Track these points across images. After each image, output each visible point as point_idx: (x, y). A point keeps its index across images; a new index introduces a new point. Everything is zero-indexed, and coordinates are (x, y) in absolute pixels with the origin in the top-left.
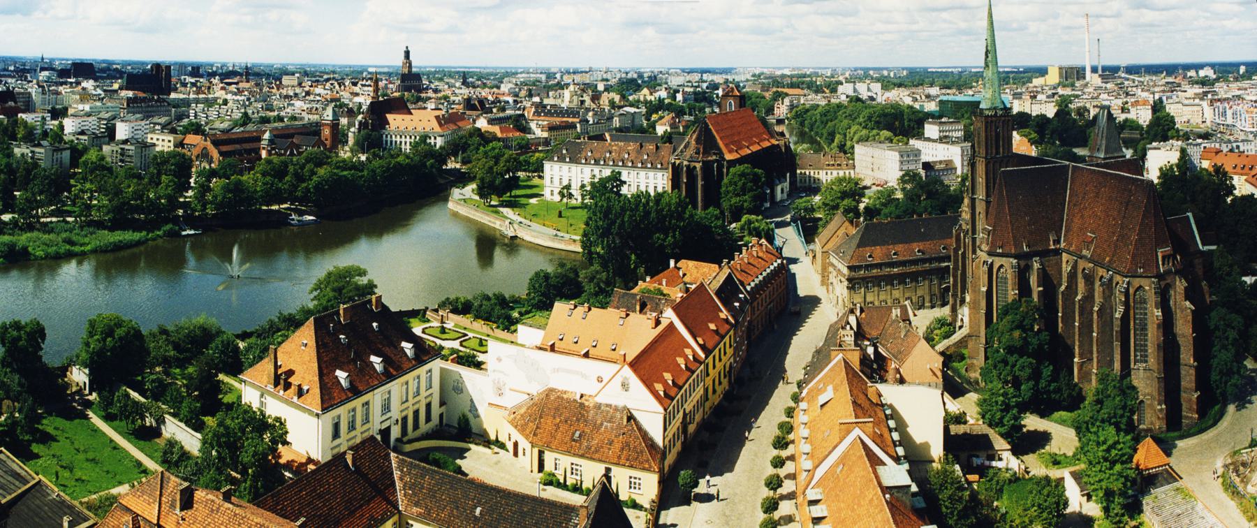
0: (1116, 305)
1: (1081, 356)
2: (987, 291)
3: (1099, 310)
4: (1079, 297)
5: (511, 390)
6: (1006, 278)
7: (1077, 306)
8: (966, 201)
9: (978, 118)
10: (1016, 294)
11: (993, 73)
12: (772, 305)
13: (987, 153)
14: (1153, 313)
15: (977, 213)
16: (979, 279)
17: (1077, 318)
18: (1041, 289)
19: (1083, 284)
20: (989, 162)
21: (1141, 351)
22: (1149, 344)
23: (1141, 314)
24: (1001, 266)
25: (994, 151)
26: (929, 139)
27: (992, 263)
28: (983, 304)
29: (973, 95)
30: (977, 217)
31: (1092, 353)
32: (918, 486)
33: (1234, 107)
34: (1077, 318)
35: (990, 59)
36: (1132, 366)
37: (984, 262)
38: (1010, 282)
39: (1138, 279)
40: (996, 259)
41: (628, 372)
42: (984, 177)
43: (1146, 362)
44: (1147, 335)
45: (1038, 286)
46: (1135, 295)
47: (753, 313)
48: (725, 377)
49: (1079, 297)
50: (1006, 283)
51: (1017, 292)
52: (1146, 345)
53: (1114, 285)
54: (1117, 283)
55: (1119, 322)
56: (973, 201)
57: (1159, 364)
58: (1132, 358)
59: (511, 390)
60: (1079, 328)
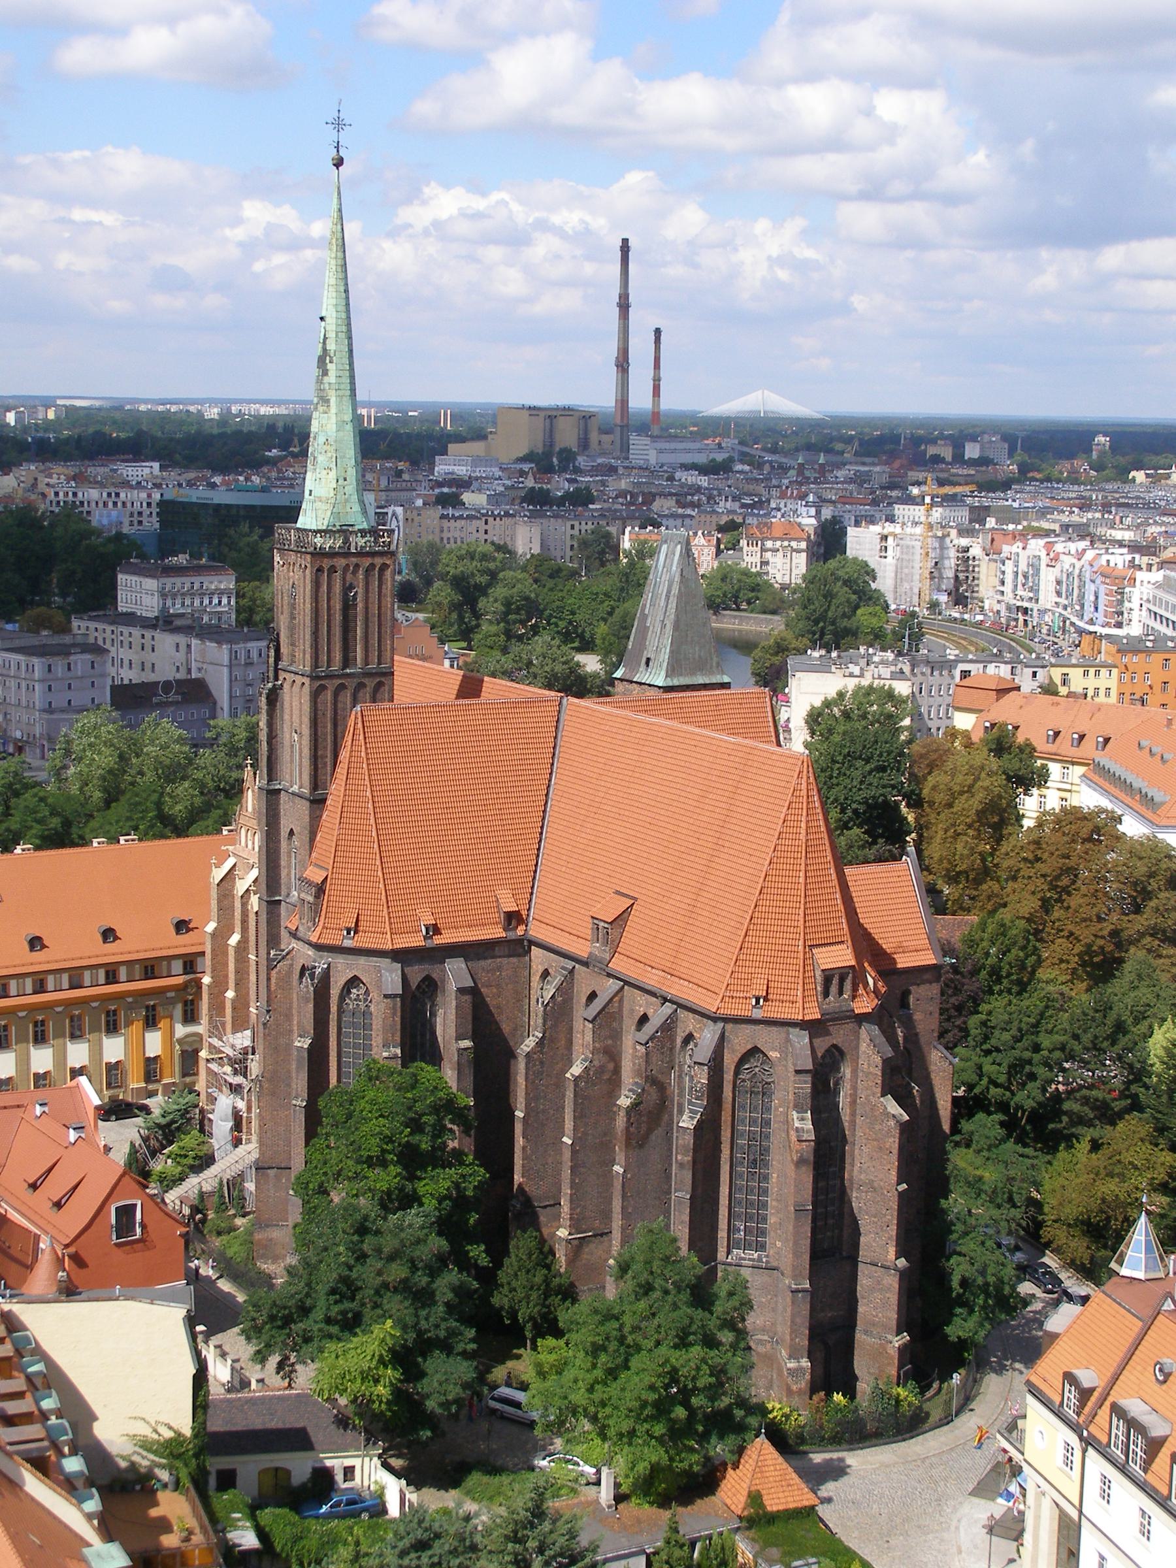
0: (681, 1095)
1: (575, 1226)
2: (311, 1050)
3: (635, 1106)
4: (576, 1070)
6: (367, 1014)
7: (570, 1094)
8: (251, 800)
9: (292, 557)
10: (395, 1057)
11: (340, 425)
13: (316, 664)
14: (788, 1122)
15: (284, 833)
16: (288, 1017)
17: (569, 1124)
18: (467, 1043)
19: (589, 1037)
20: (323, 688)
21: (748, 1218)
22: (771, 1201)
23: (753, 1122)
24: (354, 981)
25: (338, 656)
26: (130, 619)
27: (327, 973)
28: (300, 1083)
29: (264, 490)
30: (284, 844)
31: (607, 1216)
33: (1067, 561)
34: (569, 1124)
35: (332, 378)
36: (721, 1254)
37: (303, 969)
38: (377, 1023)
39: (748, 1029)
40: (339, 961)
42: (306, 731)
43: (761, 1247)
44: (766, 1178)
45: (459, 1037)
46: (737, 1072)
49: (576, 1070)
50: (367, 1027)
51: (399, 1051)
52: (765, 1205)
53: (679, 1041)
54: (689, 1038)
55: (689, 1140)
56: (272, 795)
57: (796, 1254)
58: (722, 1234)
60: (574, 1152)
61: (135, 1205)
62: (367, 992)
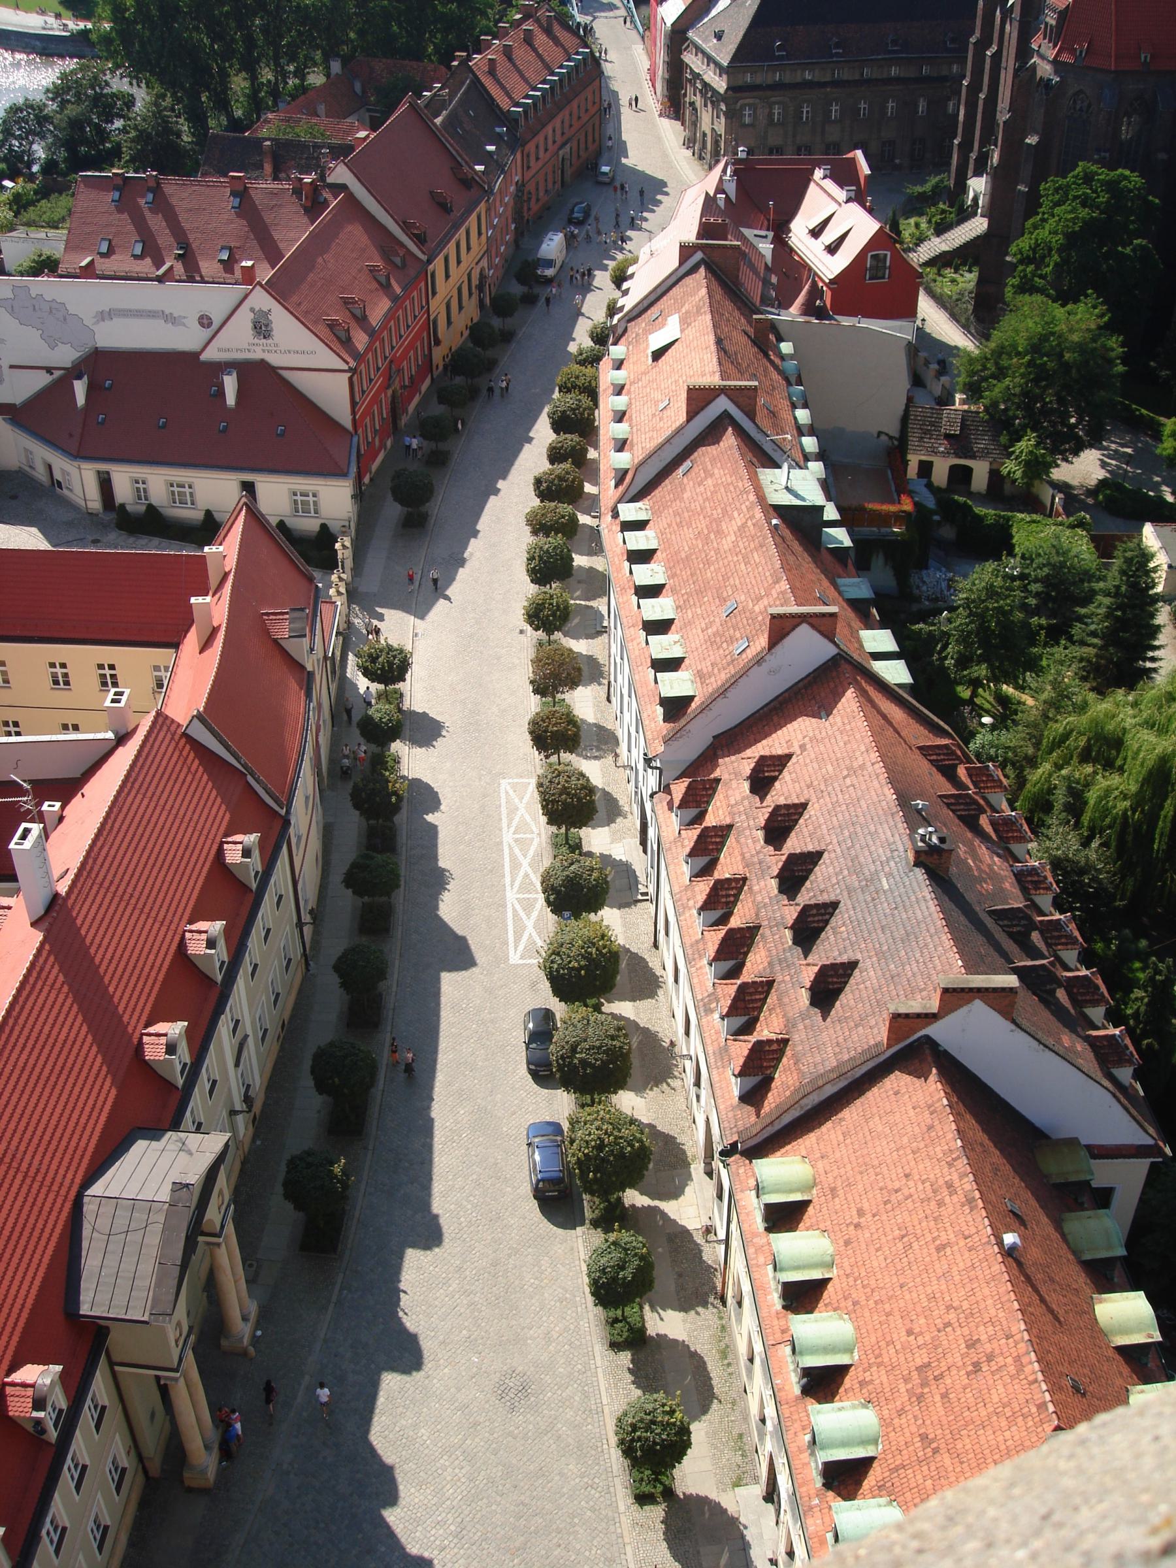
5: (12, 367)
12: (568, 147)
32: (839, 509)
41: (261, 300)
47: (526, 167)
48: (470, 294)
59: (12, 367)
61: (886, 255)
62: (1089, 106)
